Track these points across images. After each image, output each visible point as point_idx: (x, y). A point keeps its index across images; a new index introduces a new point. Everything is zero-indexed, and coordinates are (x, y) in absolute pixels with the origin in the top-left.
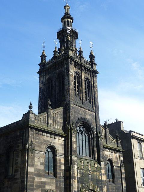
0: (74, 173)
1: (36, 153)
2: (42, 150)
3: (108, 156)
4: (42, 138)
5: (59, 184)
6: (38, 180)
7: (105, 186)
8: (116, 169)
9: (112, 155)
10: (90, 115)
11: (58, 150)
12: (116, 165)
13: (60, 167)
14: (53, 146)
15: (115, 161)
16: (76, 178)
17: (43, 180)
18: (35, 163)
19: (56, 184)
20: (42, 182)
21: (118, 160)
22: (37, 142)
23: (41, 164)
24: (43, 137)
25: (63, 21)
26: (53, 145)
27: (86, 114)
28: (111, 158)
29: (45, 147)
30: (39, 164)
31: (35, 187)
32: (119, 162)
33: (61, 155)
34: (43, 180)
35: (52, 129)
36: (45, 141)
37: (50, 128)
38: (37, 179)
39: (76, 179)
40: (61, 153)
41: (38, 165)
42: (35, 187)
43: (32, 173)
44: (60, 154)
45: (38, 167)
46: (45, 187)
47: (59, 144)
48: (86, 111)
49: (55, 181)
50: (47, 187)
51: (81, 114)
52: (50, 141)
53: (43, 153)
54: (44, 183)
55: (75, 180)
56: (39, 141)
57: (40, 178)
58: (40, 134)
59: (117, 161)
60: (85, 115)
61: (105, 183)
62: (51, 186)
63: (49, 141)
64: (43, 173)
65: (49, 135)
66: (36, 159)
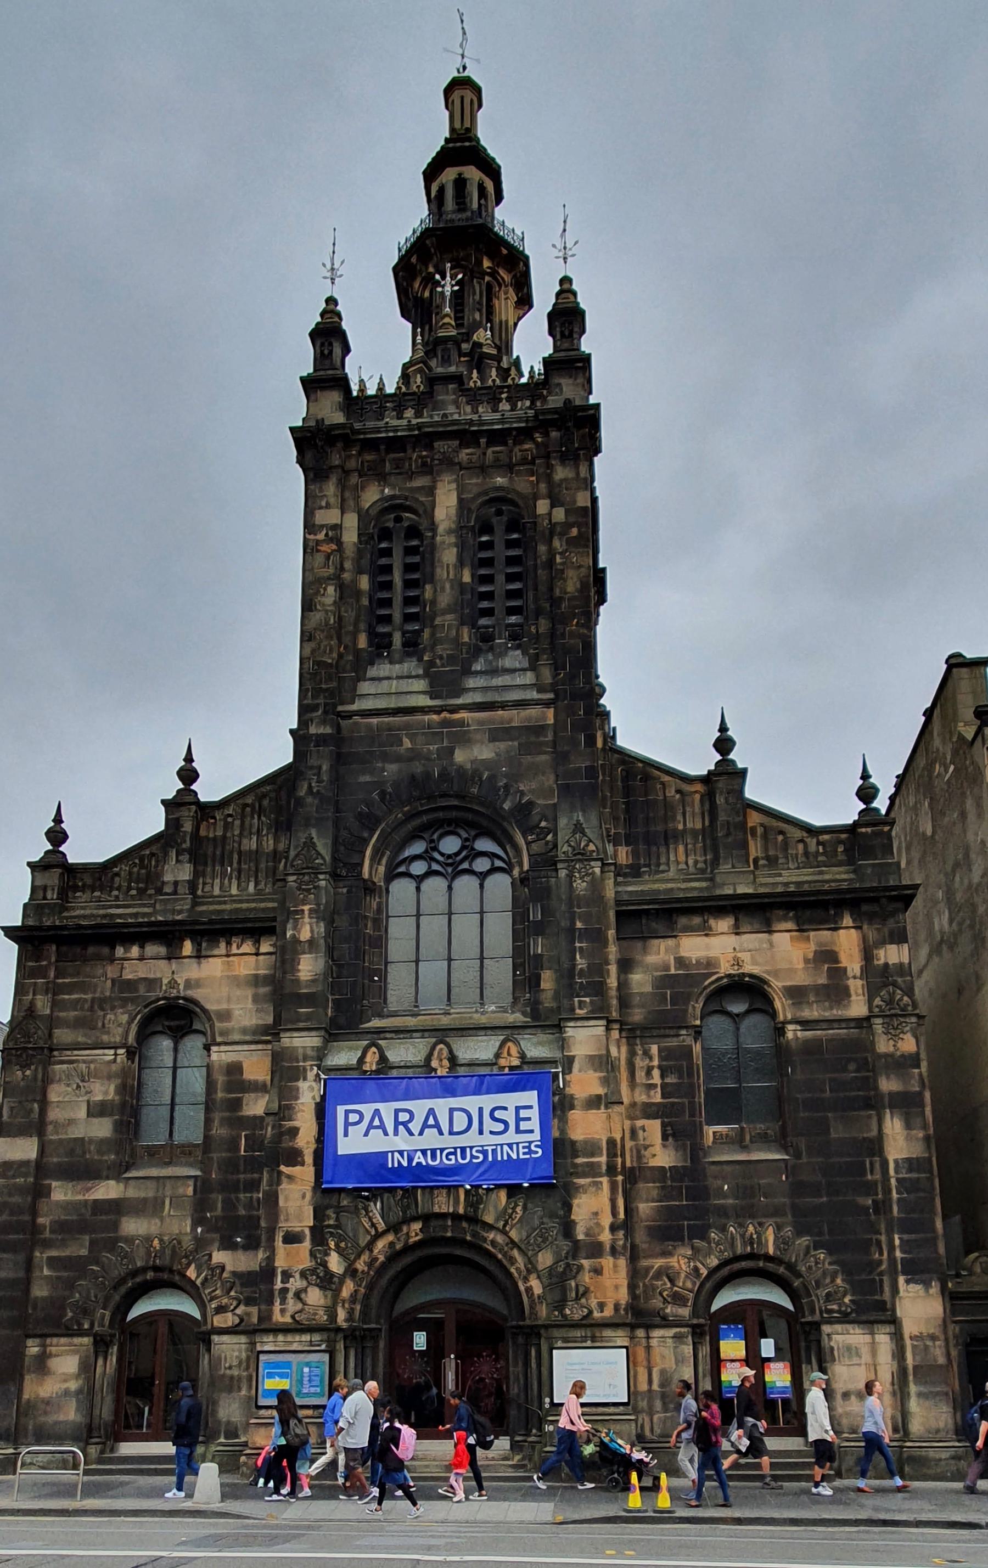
0: (294, 1132)
1: (62, 1062)
2: (105, 1038)
3: (710, 963)
4: (109, 975)
5: (219, 1205)
6: (69, 1197)
7: (605, 1180)
8: (806, 1042)
9: (771, 945)
10: (497, 734)
11: (226, 1015)
12: (812, 1012)
13: (236, 1105)
14: (184, 998)
15: (796, 994)
16: (309, 1159)
17: (108, 1190)
18: (54, 1114)
19: (200, 1206)
20: (95, 1201)
21: (838, 973)
22: (75, 1004)
23: (97, 1110)
24: (111, 971)
25: (449, 175)
26: (190, 993)
27: (462, 737)
28: (748, 968)
29: (125, 1018)
30: (82, 1113)
31: (52, 1232)
32: (856, 986)
33: (248, 1038)
34: (108, 1190)
35: (180, 912)
36: (130, 985)
37: (164, 912)
38: (61, 1192)
39: (303, 1164)
40: (244, 1031)
41: (71, 1122)
42: (47, 1234)
43: (26, 1163)
44: (237, 1037)
45: (77, 1132)
46: (116, 1226)
47: (236, 981)
48: (461, 723)
49: (190, 1191)
50: (132, 1226)
51: (414, 755)
52: (165, 981)
53: (112, 1052)
54: (116, 1208)
55: (295, 1170)
56: (89, 996)
57: (80, 1185)
58: (99, 958)
59: (822, 980)
60: (451, 751)
61: (603, 1159)
62: (162, 1219)
63: (152, 983)
64: (106, 1158)
65: (152, 949)
66: (55, 1094)
